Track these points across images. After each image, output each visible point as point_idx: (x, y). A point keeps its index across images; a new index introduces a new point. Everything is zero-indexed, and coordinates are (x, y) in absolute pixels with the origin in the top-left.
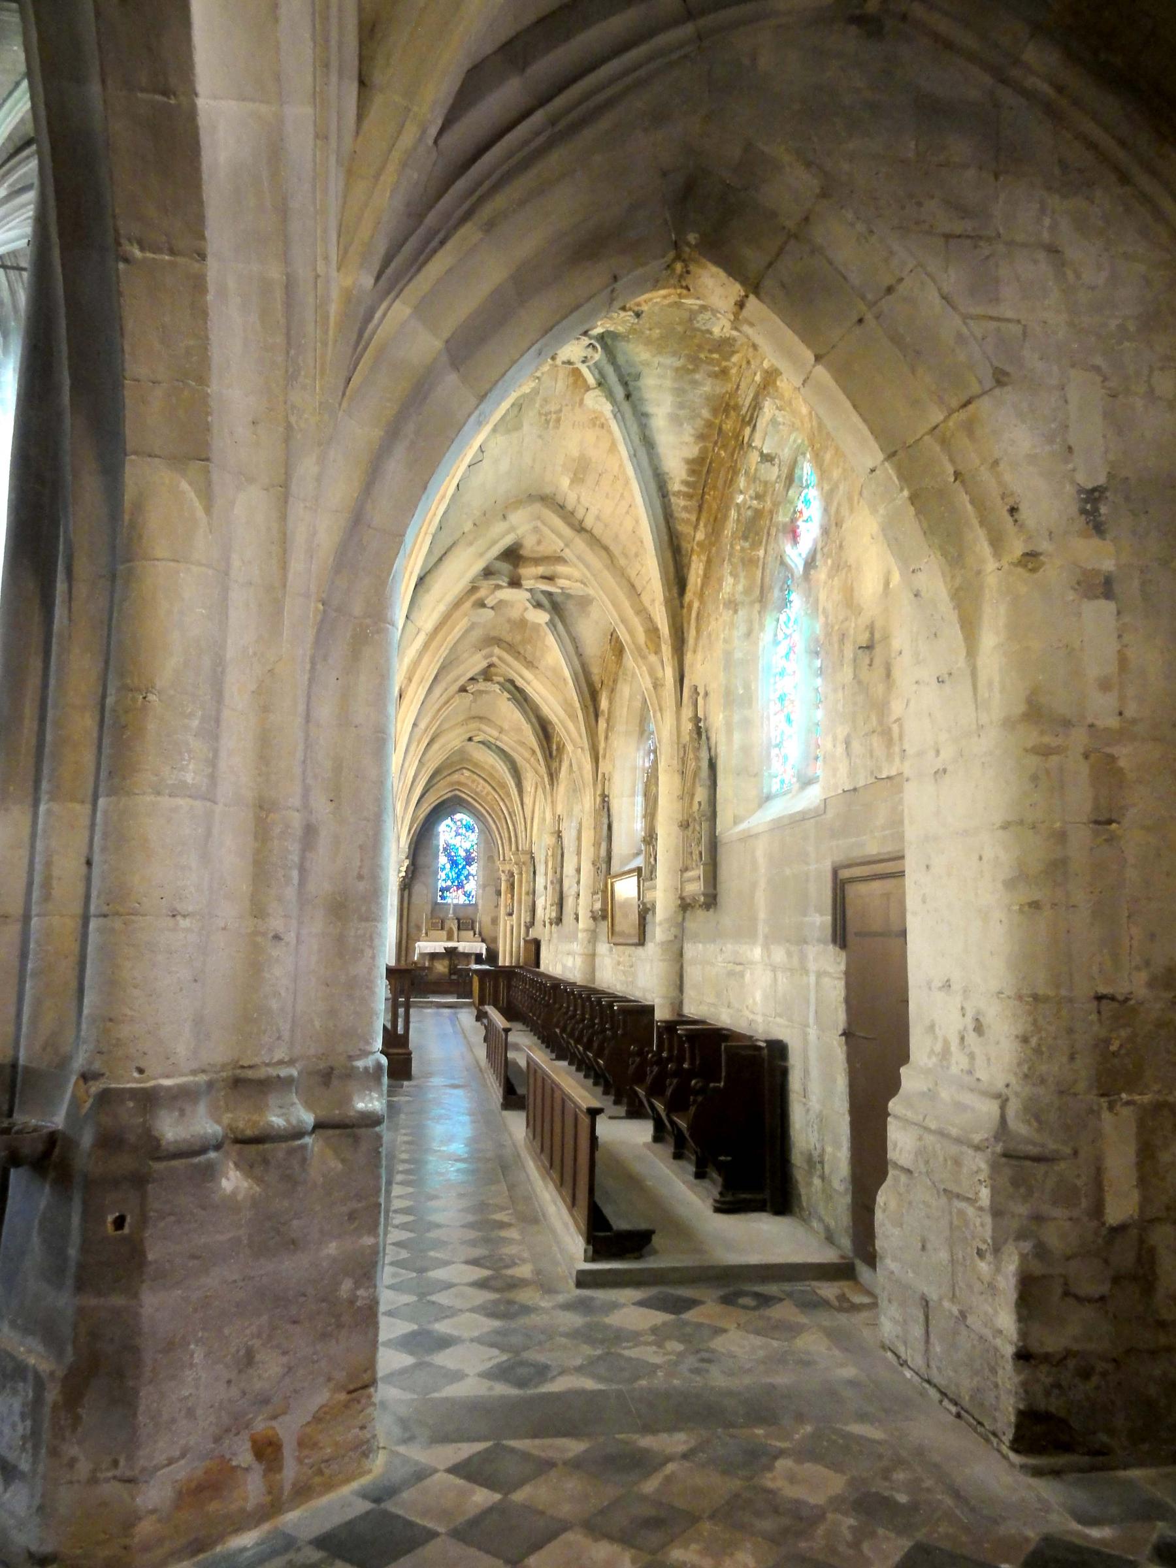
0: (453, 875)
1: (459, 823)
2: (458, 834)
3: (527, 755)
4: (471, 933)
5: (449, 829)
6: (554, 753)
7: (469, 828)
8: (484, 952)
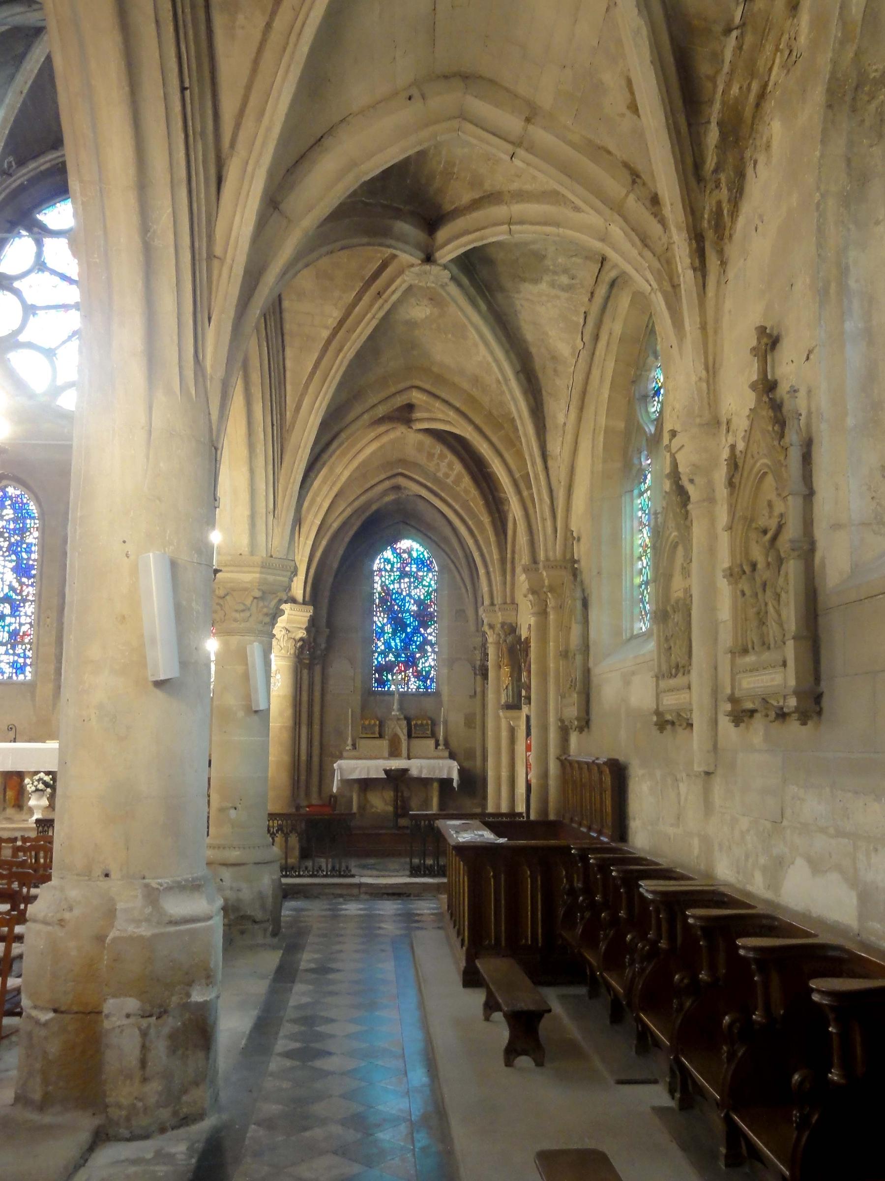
0: (396, 643)
1: (405, 556)
2: (404, 574)
3: (615, 186)
4: (432, 742)
5: (388, 567)
6: (711, 162)
8: (455, 776)
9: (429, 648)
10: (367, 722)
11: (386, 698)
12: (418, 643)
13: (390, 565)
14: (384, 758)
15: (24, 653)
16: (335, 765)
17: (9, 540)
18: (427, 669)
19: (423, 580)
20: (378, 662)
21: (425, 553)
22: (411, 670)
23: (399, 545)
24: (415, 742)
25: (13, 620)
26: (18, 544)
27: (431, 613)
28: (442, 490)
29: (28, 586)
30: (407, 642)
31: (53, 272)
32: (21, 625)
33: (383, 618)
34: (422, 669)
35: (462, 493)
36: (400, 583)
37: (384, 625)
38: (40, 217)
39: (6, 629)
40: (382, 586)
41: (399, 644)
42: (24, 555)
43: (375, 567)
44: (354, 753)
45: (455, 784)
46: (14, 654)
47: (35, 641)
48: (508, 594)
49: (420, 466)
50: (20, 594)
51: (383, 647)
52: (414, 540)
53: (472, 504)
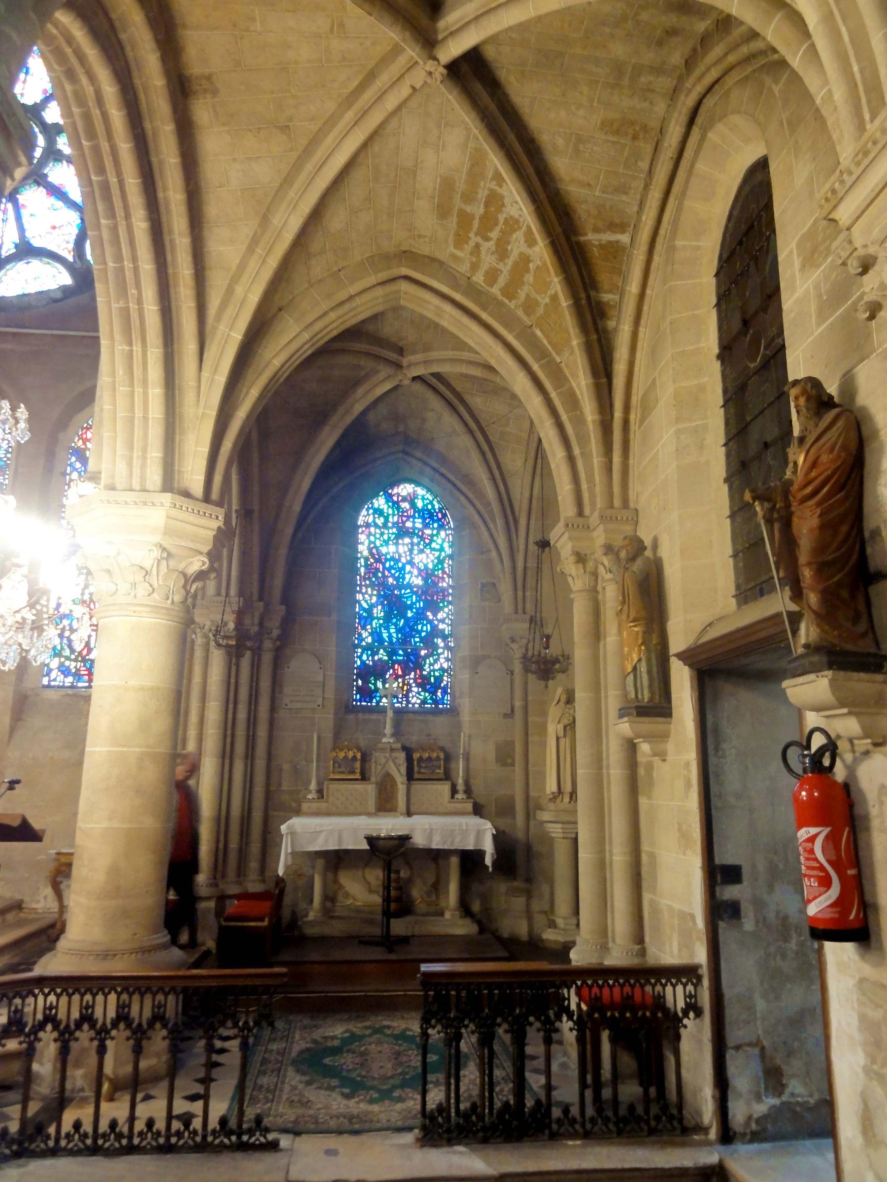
0: (391, 633)
1: (405, 505)
2: (403, 532)
4: (446, 788)
5: (380, 521)
7: (428, 516)
8: (488, 847)
9: (440, 642)
10: (342, 755)
11: (374, 717)
12: (423, 634)
13: (382, 519)
14: (369, 814)
16: (283, 828)
18: (437, 674)
19: (431, 541)
20: (363, 662)
21: (435, 503)
22: (412, 676)
23: (395, 491)
24: (416, 787)
27: (443, 590)
28: (484, 308)
30: (407, 632)
33: (371, 596)
34: (429, 673)
35: (520, 313)
36: (397, 544)
37: (372, 606)
40: (370, 550)
41: (394, 635)
43: (361, 521)
44: (323, 805)
45: (488, 861)
48: (616, 489)
49: (441, 263)
51: (369, 640)
52: (418, 484)
53: (539, 333)
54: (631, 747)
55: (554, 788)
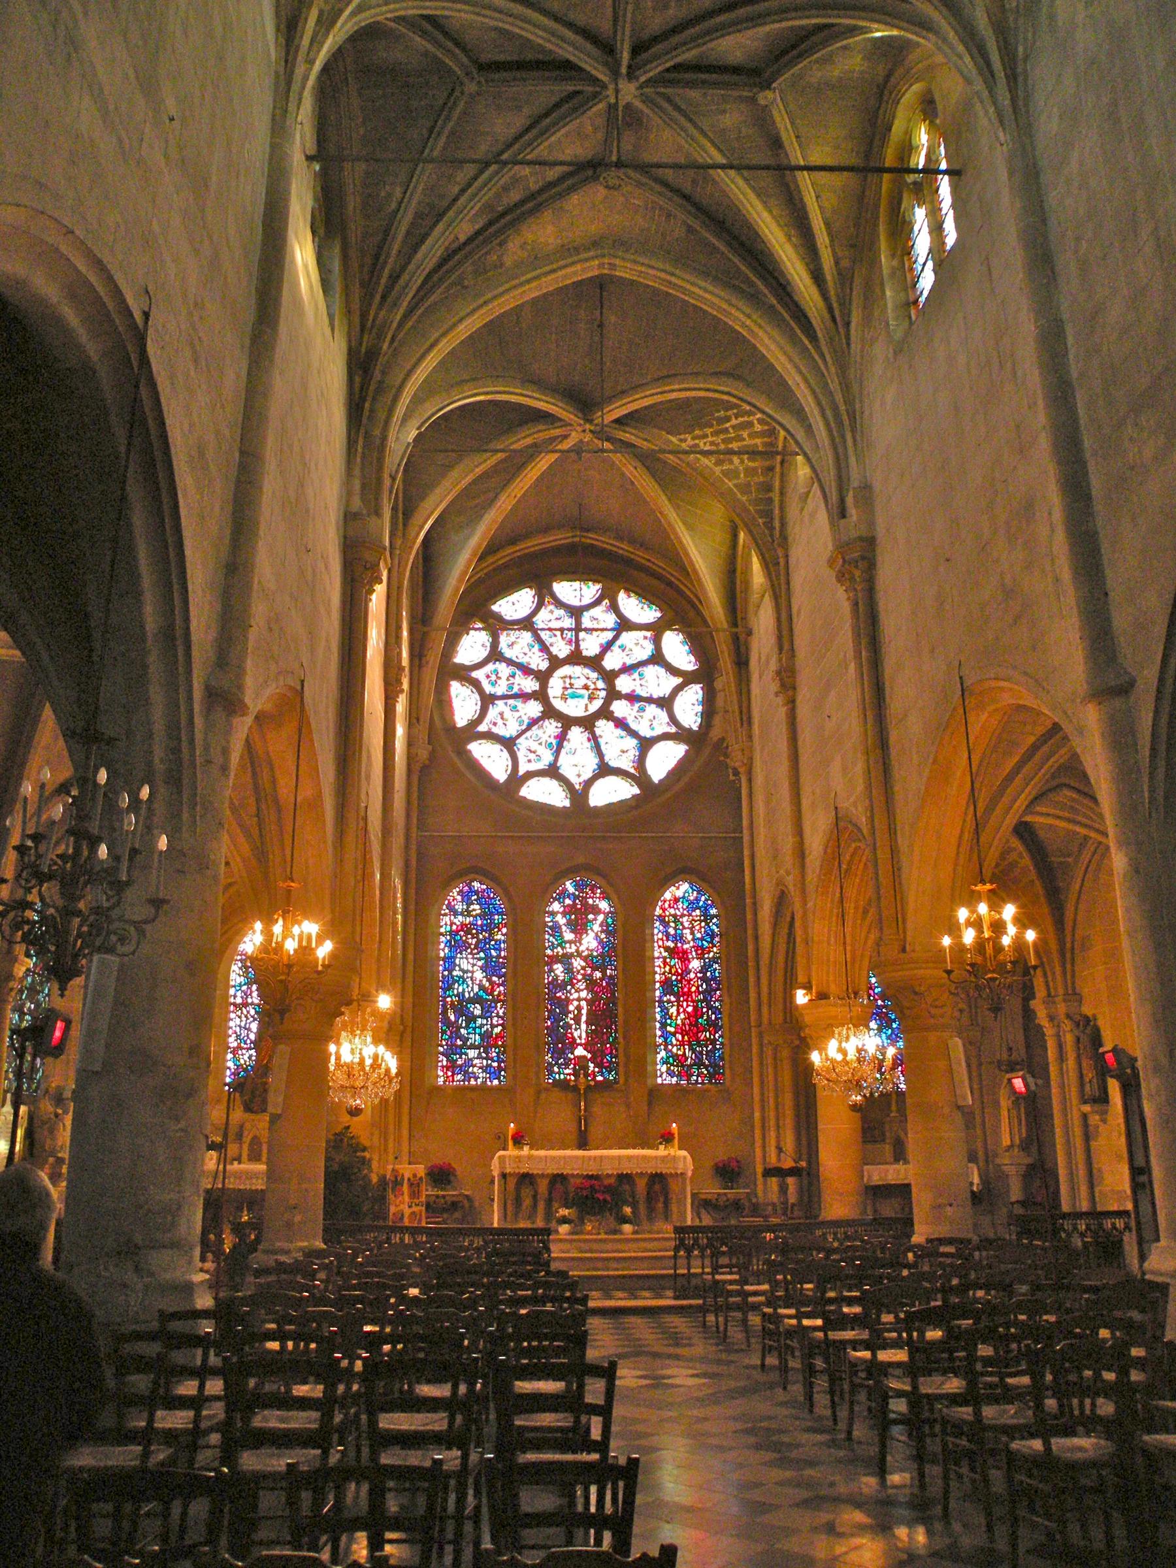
15: (498, 1056)
17: (477, 938)
25: (485, 1022)
26: (487, 941)
29: (499, 985)
31: (510, 662)
32: (493, 1026)
38: (495, 608)
39: (478, 1031)
42: (494, 953)
46: (487, 1058)
47: (509, 1042)
50: (491, 994)
54: (1085, 1117)
55: (1009, 1143)
